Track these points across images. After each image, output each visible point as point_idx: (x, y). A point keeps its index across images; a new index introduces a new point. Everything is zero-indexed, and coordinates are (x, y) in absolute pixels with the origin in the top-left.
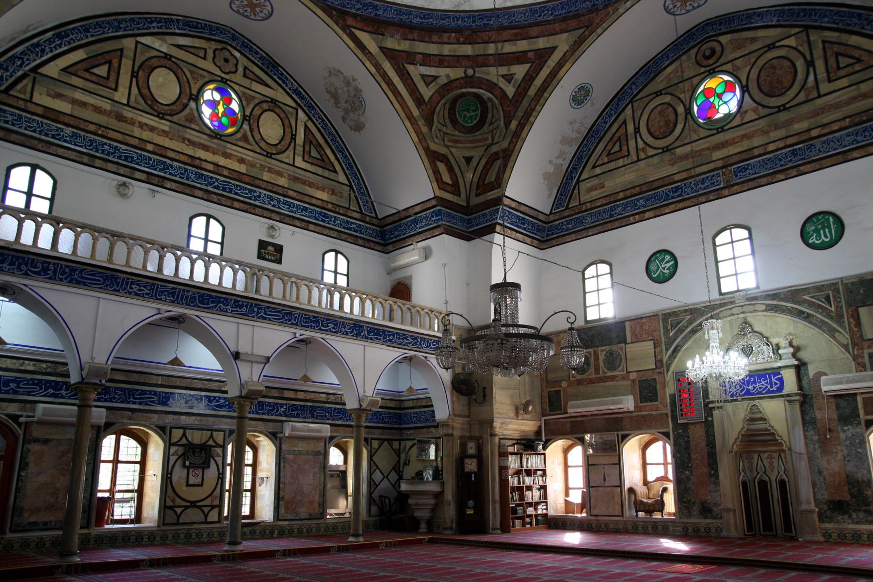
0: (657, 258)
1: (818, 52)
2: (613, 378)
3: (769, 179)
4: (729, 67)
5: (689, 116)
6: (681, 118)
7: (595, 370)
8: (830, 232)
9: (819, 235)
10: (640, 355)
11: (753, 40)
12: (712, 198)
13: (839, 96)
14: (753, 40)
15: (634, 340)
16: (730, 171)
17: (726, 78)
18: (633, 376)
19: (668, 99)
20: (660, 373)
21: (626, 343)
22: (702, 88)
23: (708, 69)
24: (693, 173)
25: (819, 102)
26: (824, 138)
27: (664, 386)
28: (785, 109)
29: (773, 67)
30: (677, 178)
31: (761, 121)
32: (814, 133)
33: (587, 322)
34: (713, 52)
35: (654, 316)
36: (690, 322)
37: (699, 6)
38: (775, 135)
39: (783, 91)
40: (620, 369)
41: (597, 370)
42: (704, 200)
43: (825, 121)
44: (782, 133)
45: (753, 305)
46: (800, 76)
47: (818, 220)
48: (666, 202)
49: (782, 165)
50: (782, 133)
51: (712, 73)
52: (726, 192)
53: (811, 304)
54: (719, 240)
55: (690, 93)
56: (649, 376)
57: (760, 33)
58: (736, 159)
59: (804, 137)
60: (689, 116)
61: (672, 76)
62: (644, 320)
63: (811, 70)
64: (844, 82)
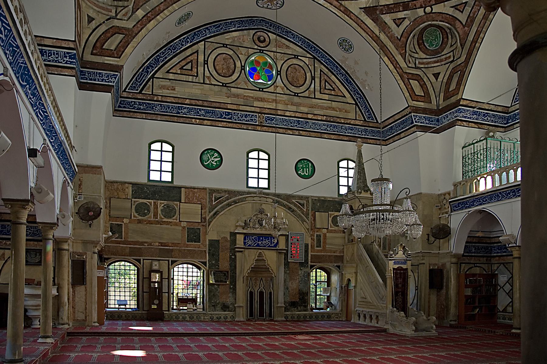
0: (209, 153)
1: (318, 74)
2: (168, 223)
3: (284, 130)
4: (272, 54)
5: (243, 71)
6: (238, 70)
7: (154, 216)
8: (309, 171)
9: (303, 171)
10: (190, 212)
11: (288, 47)
12: (250, 128)
13: (325, 103)
14: (288, 47)
15: (187, 201)
16: (263, 117)
17: (269, 60)
18: (183, 224)
19: (231, 53)
20: (203, 225)
21: (180, 202)
22: (253, 58)
23: (259, 48)
24: (242, 108)
25: (314, 100)
26: (314, 121)
27: (206, 233)
28: (297, 96)
29: (295, 69)
30: (229, 106)
31: (285, 96)
32: (310, 116)
33: (149, 180)
34: (265, 40)
35: (205, 189)
36: (227, 199)
37: (270, 9)
38: (290, 108)
39: (299, 85)
40: (174, 218)
41: (155, 215)
42: (245, 128)
43: (315, 112)
44: (294, 108)
45: (267, 198)
46: (308, 82)
47: (304, 163)
48: (220, 119)
49: (291, 126)
50: (294, 108)
51: (261, 51)
52: (259, 128)
53: (295, 205)
54: (251, 155)
55: (246, 57)
56: (196, 226)
57: (291, 45)
58: (267, 111)
59: (305, 116)
60: (243, 71)
61: (236, 39)
62: (196, 190)
63: (313, 81)
64: (326, 97)
